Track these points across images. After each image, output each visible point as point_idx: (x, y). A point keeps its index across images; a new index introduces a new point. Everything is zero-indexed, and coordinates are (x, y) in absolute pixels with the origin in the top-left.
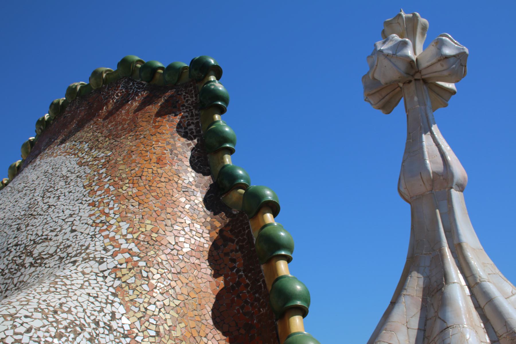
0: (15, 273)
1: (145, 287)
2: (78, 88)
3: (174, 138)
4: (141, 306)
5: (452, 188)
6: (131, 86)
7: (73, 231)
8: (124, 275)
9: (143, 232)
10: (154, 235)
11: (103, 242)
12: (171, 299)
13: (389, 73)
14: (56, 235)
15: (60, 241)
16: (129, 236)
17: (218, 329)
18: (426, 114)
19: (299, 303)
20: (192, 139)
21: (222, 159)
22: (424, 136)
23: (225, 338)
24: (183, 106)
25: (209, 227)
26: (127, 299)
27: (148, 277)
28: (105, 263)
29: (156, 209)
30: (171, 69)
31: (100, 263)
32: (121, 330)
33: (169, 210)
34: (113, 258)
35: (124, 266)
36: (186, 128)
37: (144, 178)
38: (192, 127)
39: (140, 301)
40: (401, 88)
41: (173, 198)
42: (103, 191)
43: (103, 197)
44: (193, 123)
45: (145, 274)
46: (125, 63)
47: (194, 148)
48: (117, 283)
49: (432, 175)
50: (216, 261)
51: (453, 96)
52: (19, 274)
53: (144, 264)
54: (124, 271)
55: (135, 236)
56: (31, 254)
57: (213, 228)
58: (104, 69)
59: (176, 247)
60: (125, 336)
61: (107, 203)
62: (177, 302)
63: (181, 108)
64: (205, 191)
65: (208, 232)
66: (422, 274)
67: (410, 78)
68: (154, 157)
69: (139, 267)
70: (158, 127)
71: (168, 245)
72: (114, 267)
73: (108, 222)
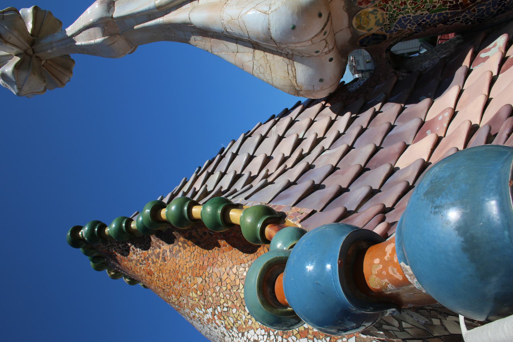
1: (234, 310)
2: (127, 280)
3: (132, 260)
5: (112, 17)
8: (229, 325)
10: (199, 292)
12: (239, 291)
13: (34, 83)
17: (256, 251)
18: (59, 41)
19: (219, 212)
20: (129, 247)
21: (135, 231)
22: (78, 43)
23: (262, 247)
24: (108, 250)
25: (186, 245)
26: (244, 326)
27: (227, 307)
29: (181, 286)
30: (86, 253)
31: (225, 335)
32: (266, 337)
33: (180, 276)
35: (223, 322)
36: (123, 250)
37: (163, 288)
38: (120, 246)
39: (244, 317)
40: (47, 60)
41: (172, 270)
44: (118, 245)
45: (225, 309)
46: (98, 268)
47: (135, 246)
48: (235, 329)
49: (106, 37)
51: (42, 8)
53: (219, 308)
54: (227, 323)
55: (202, 307)
57: (185, 243)
58: (109, 275)
59: (204, 277)
60: (269, 335)
62: (241, 286)
64: (161, 242)
65: (189, 247)
66: (191, 37)
67: (34, 60)
68: (148, 277)
70: (128, 268)
71: (204, 283)
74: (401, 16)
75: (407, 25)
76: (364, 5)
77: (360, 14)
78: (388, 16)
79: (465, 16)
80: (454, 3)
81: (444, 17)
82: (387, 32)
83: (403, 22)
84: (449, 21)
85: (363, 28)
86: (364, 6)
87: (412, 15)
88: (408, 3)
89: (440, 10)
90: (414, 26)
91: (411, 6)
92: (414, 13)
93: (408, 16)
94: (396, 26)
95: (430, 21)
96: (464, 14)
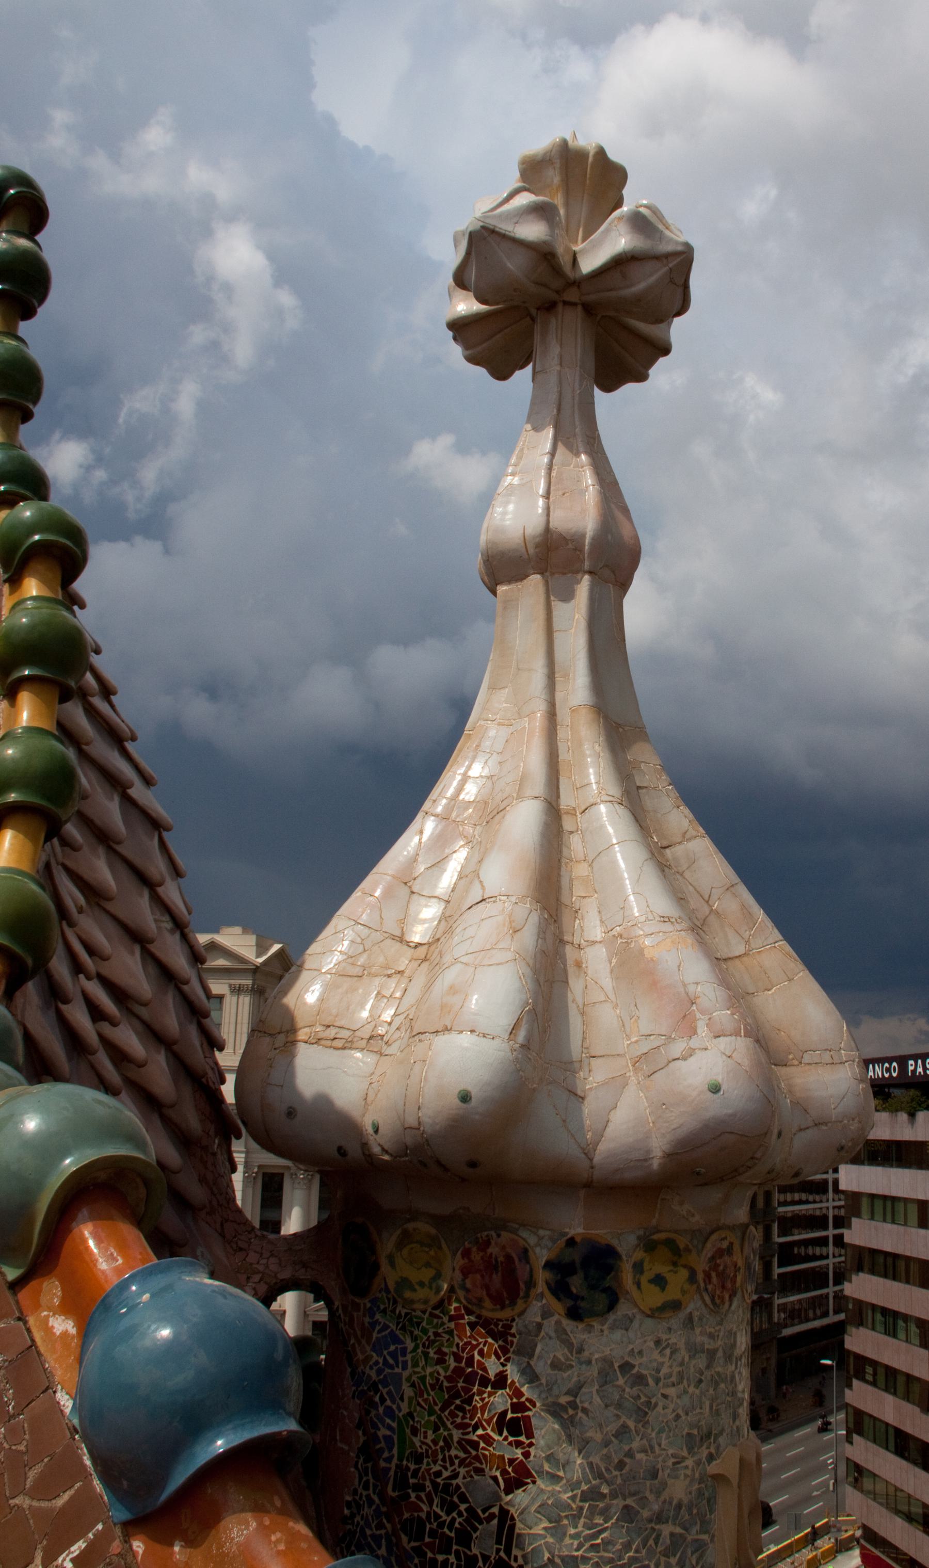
74: (410, 1345)
75: (380, 1354)
76: (462, 1262)
77: (440, 1248)
78: (419, 1313)
79: (371, 1502)
80: (412, 1481)
81: (381, 1451)
82: (374, 1301)
83: (392, 1348)
84: (365, 1461)
85: (400, 1245)
86: (459, 1261)
87: (405, 1374)
88: (438, 1368)
89: (402, 1441)
90: (373, 1374)
91: (431, 1374)
92: (408, 1379)
93: (405, 1364)
94: (386, 1327)
95: (377, 1416)
96: (377, 1500)
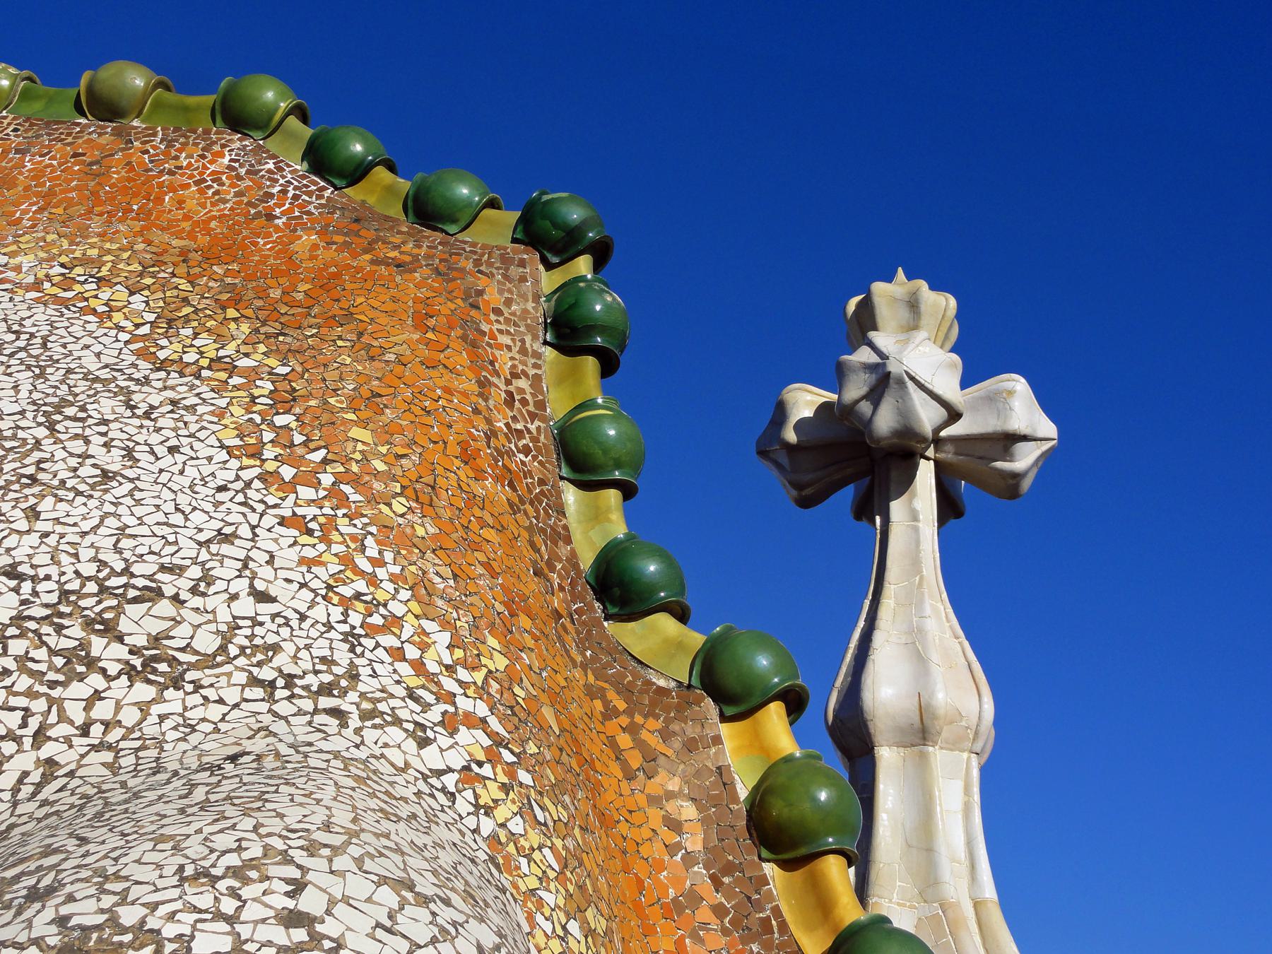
0: (64, 684)
4: (554, 914)
6: (269, 171)
7: (263, 597)
9: (490, 672)
11: (395, 671)
14: (194, 591)
15: (224, 615)
16: (463, 674)
28: (433, 748)
34: (451, 735)
38: (523, 383)
42: (322, 493)
43: (327, 511)
50: (630, 812)
52: (80, 690)
55: (479, 677)
56: (110, 631)
61: (353, 538)
63: (493, 317)
69: (521, 784)
72: (467, 768)
73: (385, 605)
